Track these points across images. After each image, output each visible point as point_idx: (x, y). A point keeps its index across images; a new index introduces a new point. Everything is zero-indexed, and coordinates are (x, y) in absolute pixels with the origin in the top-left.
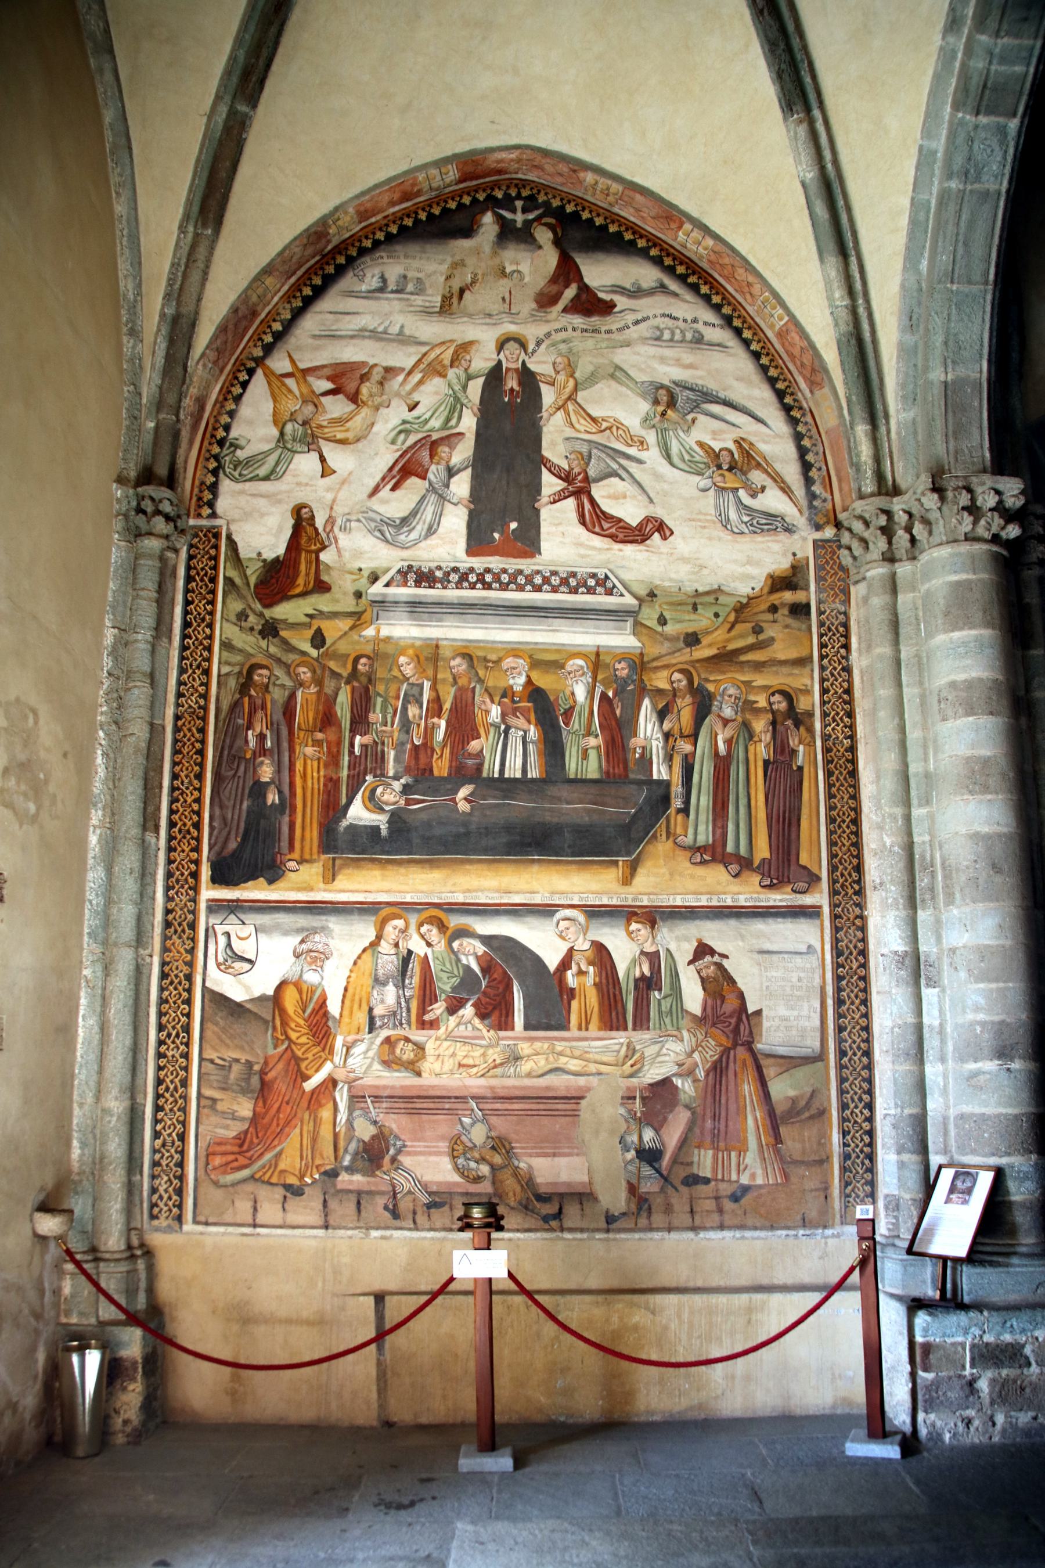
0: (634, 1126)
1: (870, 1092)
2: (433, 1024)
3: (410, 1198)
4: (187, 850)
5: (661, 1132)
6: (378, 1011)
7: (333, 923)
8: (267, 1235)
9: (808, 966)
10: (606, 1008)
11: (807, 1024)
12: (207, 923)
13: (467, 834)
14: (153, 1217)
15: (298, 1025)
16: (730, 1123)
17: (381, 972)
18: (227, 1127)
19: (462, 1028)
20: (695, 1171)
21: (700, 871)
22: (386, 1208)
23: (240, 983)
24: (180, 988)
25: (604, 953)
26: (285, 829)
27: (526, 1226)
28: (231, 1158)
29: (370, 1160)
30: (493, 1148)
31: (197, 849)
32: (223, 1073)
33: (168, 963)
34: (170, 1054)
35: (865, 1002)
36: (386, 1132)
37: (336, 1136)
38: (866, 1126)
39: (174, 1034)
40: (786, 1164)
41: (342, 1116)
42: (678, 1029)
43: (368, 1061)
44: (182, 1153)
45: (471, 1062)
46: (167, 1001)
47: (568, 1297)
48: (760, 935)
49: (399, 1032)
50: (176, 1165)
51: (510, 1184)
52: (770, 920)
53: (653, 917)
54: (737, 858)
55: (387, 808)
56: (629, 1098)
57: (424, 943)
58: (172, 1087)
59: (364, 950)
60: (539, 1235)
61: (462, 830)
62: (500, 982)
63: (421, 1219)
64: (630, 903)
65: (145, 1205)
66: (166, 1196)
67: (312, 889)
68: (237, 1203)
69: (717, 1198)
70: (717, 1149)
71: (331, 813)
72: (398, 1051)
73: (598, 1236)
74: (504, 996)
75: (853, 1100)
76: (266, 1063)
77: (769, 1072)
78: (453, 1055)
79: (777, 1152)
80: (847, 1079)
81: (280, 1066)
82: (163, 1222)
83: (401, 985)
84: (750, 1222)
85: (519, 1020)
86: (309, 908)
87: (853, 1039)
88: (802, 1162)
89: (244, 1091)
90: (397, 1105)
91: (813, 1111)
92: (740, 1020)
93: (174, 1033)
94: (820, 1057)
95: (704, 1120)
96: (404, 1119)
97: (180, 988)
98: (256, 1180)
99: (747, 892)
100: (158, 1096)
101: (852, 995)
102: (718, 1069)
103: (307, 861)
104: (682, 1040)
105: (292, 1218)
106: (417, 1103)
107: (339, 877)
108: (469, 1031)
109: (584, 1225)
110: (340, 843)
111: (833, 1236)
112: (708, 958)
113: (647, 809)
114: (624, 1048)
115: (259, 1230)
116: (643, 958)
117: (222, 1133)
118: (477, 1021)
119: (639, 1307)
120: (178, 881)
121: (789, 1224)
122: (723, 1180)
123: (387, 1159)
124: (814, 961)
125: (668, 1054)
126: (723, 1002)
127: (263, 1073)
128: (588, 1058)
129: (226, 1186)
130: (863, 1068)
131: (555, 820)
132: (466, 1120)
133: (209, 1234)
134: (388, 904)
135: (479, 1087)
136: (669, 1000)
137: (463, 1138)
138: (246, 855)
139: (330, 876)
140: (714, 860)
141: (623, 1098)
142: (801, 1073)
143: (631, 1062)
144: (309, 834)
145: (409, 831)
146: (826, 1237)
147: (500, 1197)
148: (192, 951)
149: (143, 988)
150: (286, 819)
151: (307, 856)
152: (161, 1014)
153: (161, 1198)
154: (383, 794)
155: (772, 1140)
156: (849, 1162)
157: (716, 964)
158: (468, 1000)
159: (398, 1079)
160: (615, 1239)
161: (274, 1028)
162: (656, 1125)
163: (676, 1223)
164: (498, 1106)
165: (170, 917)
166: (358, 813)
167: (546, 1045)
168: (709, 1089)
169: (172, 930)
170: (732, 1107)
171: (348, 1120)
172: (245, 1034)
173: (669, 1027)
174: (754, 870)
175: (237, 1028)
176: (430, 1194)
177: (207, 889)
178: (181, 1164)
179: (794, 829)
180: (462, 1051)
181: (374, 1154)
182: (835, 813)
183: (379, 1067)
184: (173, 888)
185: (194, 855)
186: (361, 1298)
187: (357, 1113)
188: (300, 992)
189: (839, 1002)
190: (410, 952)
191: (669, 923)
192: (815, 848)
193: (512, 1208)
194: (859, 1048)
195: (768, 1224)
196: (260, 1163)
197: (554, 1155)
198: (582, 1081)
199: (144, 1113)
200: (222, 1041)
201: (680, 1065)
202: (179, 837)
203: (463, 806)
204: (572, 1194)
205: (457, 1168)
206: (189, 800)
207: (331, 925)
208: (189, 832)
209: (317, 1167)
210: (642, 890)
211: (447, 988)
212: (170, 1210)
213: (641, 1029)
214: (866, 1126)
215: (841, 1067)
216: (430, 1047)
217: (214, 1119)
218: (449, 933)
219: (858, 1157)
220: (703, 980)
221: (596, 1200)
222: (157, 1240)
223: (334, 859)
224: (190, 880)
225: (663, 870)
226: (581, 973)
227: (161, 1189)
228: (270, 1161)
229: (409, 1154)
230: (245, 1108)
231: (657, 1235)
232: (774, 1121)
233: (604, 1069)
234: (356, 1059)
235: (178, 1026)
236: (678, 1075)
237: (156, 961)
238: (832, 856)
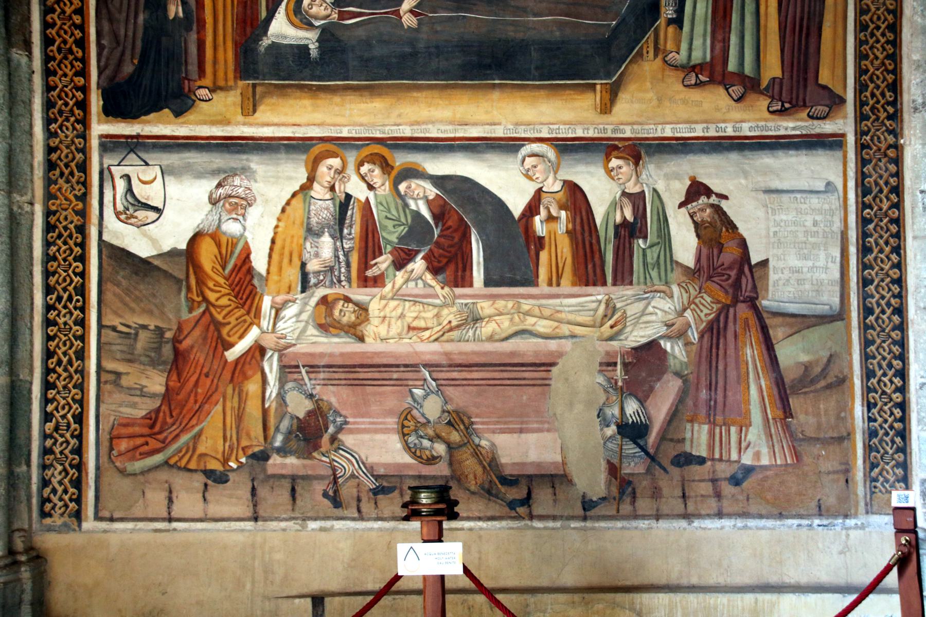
0: (614, 398)
1: (903, 357)
2: (378, 281)
3: (354, 482)
4: (70, 74)
5: (647, 404)
6: (313, 266)
7: (256, 163)
8: (185, 530)
9: (826, 207)
10: (582, 260)
11: (823, 276)
12: (101, 164)
13: (414, 54)
14: (44, 514)
15: (217, 284)
16: (729, 394)
17: (314, 220)
18: (134, 405)
19: (411, 284)
20: (687, 448)
21: (695, 95)
22: (325, 495)
23: (145, 235)
24: (71, 243)
25: (579, 195)
26: (193, 49)
27: (489, 514)
28: (139, 441)
29: (306, 440)
30: (449, 423)
31: (84, 73)
32: (128, 341)
33: (54, 213)
34: (61, 321)
35: (898, 250)
36: (325, 407)
37: (265, 412)
38: (897, 397)
39: (66, 295)
40: (797, 443)
41: (272, 390)
42: (667, 283)
43: (303, 324)
44: (80, 437)
45: (422, 324)
46: (55, 258)
47: (539, 596)
48: (768, 171)
50: (72, 452)
51: (470, 465)
52: (780, 153)
53: (636, 151)
54: (740, 77)
55: (317, 23)
56: (609, 364)
57: (364, 186)
58: (65, 360)
59: (294, 195)
60: (504, 523)
61: (407, 50)
62: (456, 231)
63: (366, 507)
64: (609, 134)
65: (34, 501)
66: (60, 489)
67: (227, 122)
68: (149, 495)
69: (714, 481)
70: (713, 424)
71: (249, 30)
72: (336, 313)
73: (574, 524)
74: (461, 248)
75: (880, 367)
76: (180, 329)
77: (777, 333)
78: (402, 316)
79: (787, 427)
80: (873, 342)
81: (197, 333)
82: (57, 520)
83: (338, 236)
84: (753, 509)
85: (478, 274)
86: (227, 146)
87: (881, 294)
88: (818, 439)
89: (154, 363)
90: (336, 376)
91: (831, 379)
92: (741, 272)
93: (65, 296)
94: (841, 315)
95: (697, 389)
96: (345, 392)
97: (71, 243)
98: (171, 466)
99: (753, 119)
100: (47, 371)
101: (881, 242)
102: (715, 331)
103: (221, 89)
104: (671, 297)
105: (214, 509)
106: (361, 373)
107: (261, 108)
108: (420, 289)
109: (557, 512)
110: (260, 67)
111: (856, 527)
112: (703, 200)
113: (631, 20)
114: (603, 306)
115: (175, 525)
116: (625, 200)
117: (127, 411)
118: (428, 277)
119: (623, 608)
120: (61, 112)
121: (802, 512)
122: (721, 460)
123: (326, 438)
124: (834, 201)
125: (655, 313)
126: (720, 252)
127: (176, 341)
128: (559, 316)
129: (135, 475)
130: (893, 329)
131: (520, 36)
132: (418, 392)
133: (115, 531)
134: (322, 139)
135: (434, 353)
136: (656, 249)
137: (415, 412)
138: (146, 82)
139: (250, 107)
140: (712, 81)
141: (601, 364)
142: (816, 334)
143: (611, 322)
144: (222, 54)
145: (344, 51)
146: (848, 529)
147: (459, 480)
148: (84, 198)
149: (22, 241)
150: (193, 36)
151: (221, 83)
152: (47, 274)
153: (54, 491)
154: (311, 5)
155: (780, 413)
156: (875, 440)
157: (712, 206)
158: (417, 252)
159: (337, 346)
160: (593, 529)
161: (189, 289)
162: (640, 395)
163: (665, 509)
164: (455, 375)
165: (54, 156)
166: (282, 29)
167: (510, 304)
168: (704, 353)
169: (57, 172)
170: (732, 374)
171: (279, 394)
172: (154, 295)
173: (656, 281)
174: (761, 93)
175: (143, 288)
176: (377, 477)
177: (99, 122)
178: (79, 451)
179: (813, 40)
180: (411, 312)
181: (311, 432)
182: (867, 18)
183: (315, 332)
184: (56, 121)
185: (80, 81)
186: (297, 601)
187: (290, 385)
188: (219, 245)
189: (864, 250)
190: (348, 197)
191: (656, 157)
192: (840, 62)
193: (473, 493)
194: (889, 304)
195: (776, 512)
196: (175, 446)
197: (521, 431)
198: (553, 345)
199: (30, 391)
200: (126, 304)
201: (669, 326)
202: (59, 57)
203: (409, 20)
204: (543, 476)
205: (407, 447)
206: (68, 11)
207: (253, 166)
208: (70, 51)
209: (243, 449)
210: (624, 118)
211: (394, 238)
212: (66, 506)
213: (623, 283)
214: (897, 397)
215: (865, 327)
216: (374, 307)
217: (118, 396)
218: (394, 173)
219: (887, 434)
220: (697, 225)
221: (570, 482)
222: (49, 541)
223: (254, 86)
224: (77, 112)
225: (650, 95)
226: (551, 218)
227: (55, 481)
228: (187, 444)
229: (351, 432)
230: (156, 383)
231: (643, 524)
232: (783, 392)
233: (578, 330)
234: (287, 323)
235: (71, 288)
236: (666, 337)
237: (38, 209)
238: (861, 71)
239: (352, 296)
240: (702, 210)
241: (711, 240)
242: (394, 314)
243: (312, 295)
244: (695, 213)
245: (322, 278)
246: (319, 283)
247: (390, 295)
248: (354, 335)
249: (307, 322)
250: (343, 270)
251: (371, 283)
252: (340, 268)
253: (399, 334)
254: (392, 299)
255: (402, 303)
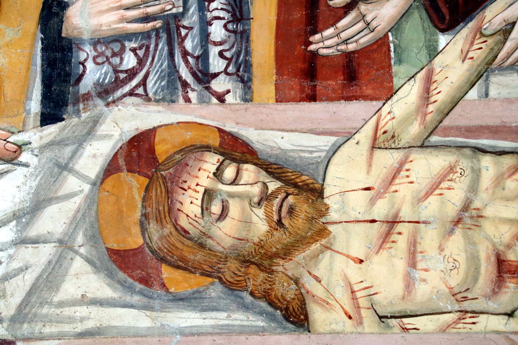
2: (361, 74)
43: (47, 251)
49: (194, 112)
72: (190, 204)
78: (466, 217)
183: (98, 286)
216: (349, 181)
239: (252, 136)
242: (431, 207)
243: (90, 131)
245: (130, 61)
246: (118, 83)
247: (415, 129)
248: (267, 297)
249: (65, 244)
250: (217, 31)
251: (335, 83)
252: (205, 24)
253: (460, 295)
254: (423, 146)
255: (465, 163)
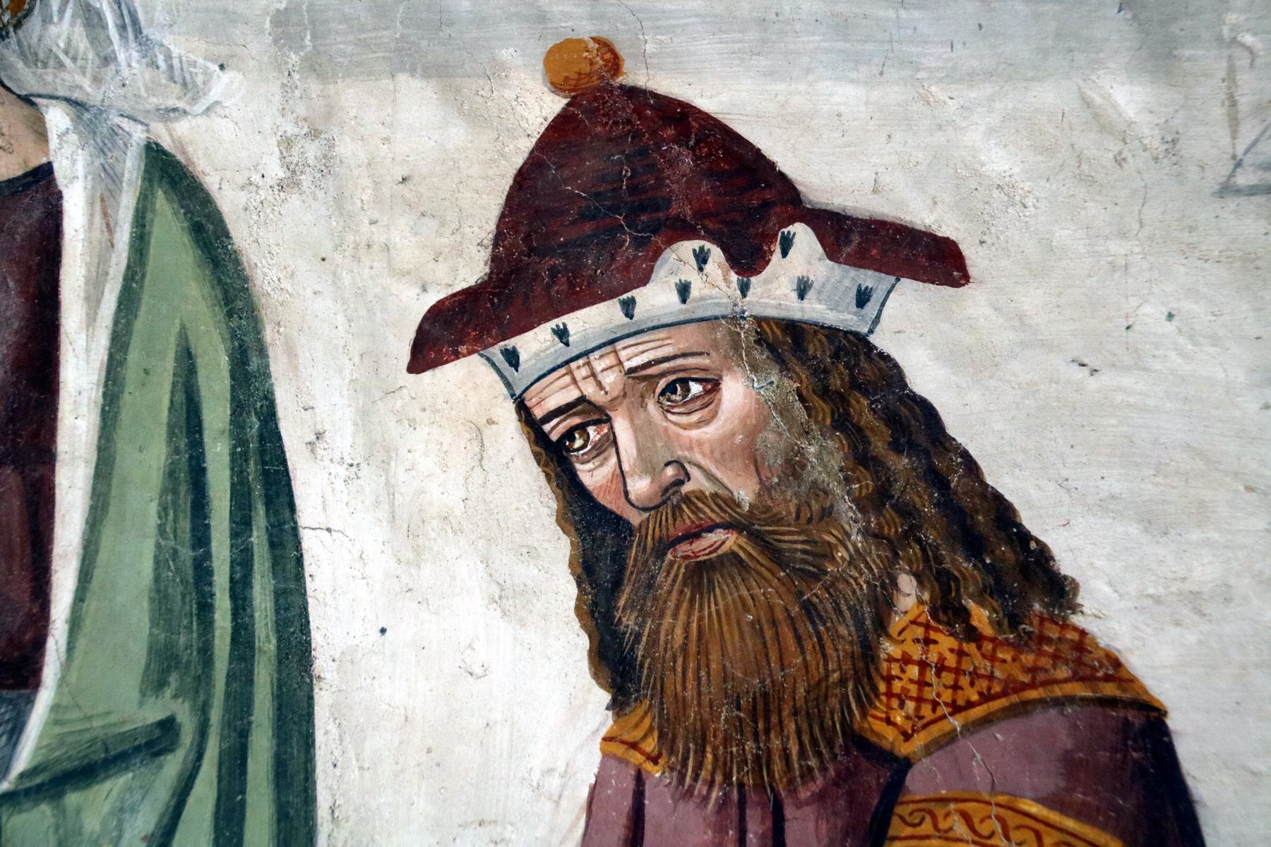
112: (686, 281)
157: (785, 341)
220: (602, 544)
240: (677, 386)
241: (762, 709)
244: (591, 412)
